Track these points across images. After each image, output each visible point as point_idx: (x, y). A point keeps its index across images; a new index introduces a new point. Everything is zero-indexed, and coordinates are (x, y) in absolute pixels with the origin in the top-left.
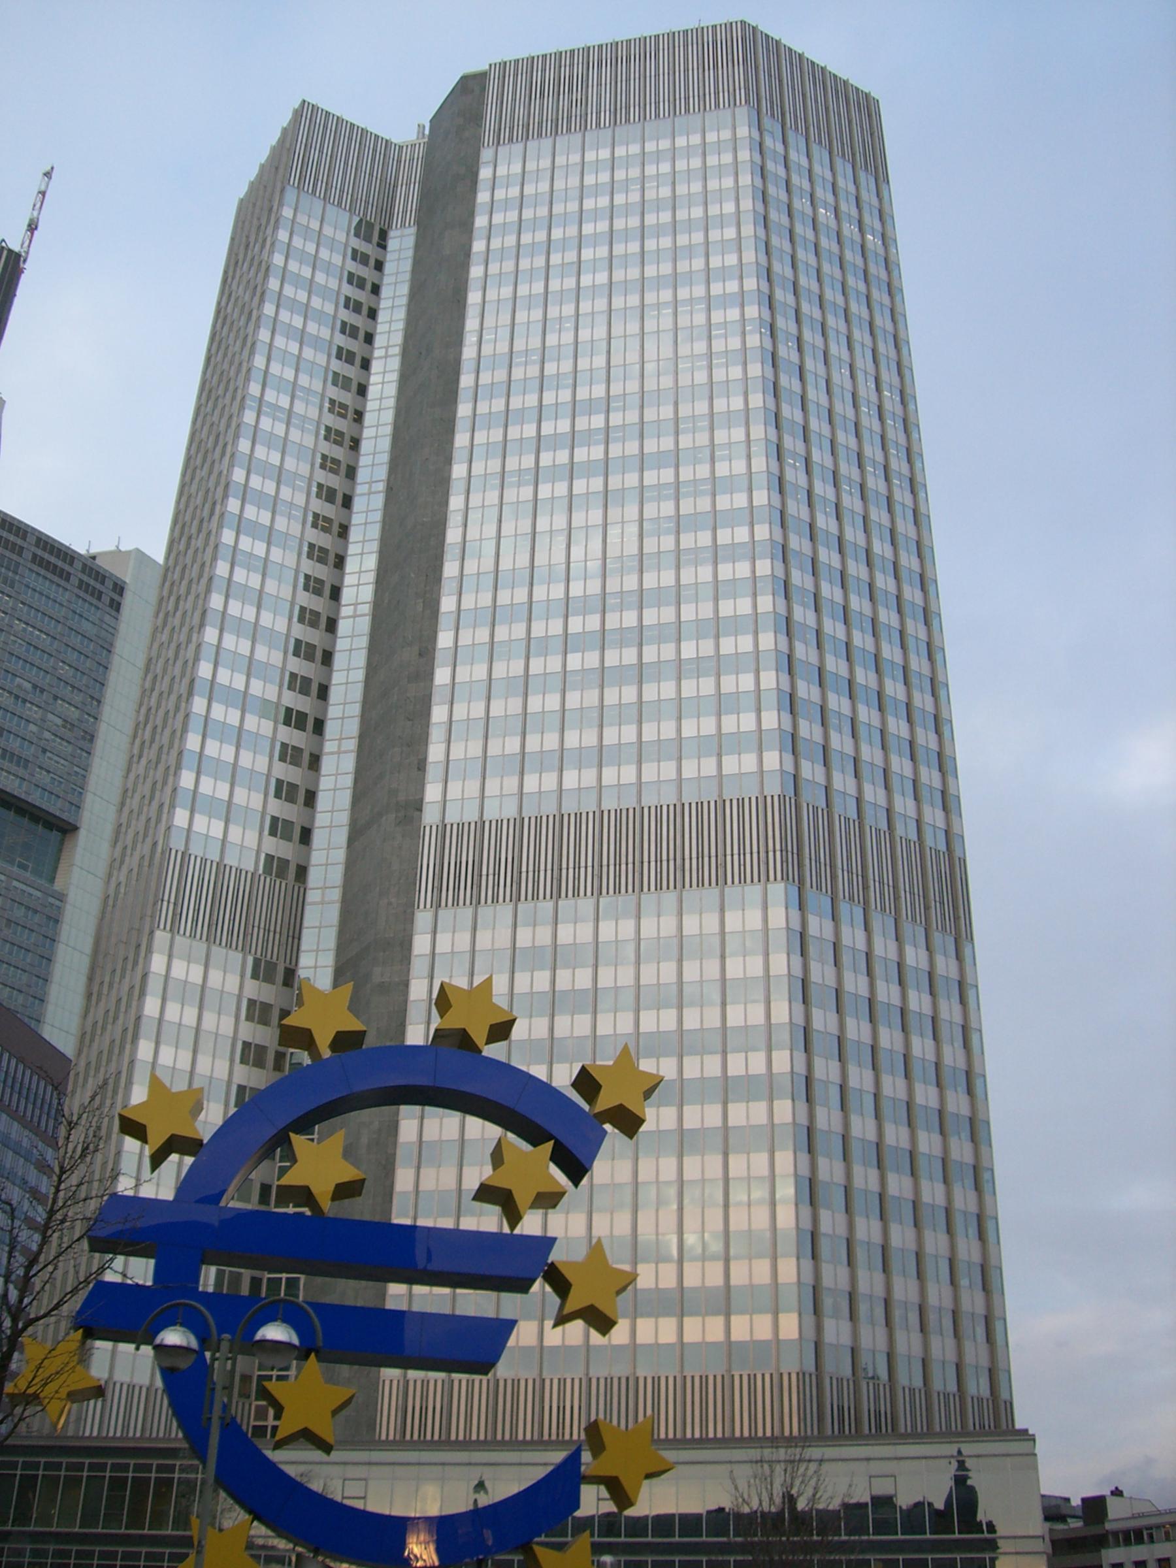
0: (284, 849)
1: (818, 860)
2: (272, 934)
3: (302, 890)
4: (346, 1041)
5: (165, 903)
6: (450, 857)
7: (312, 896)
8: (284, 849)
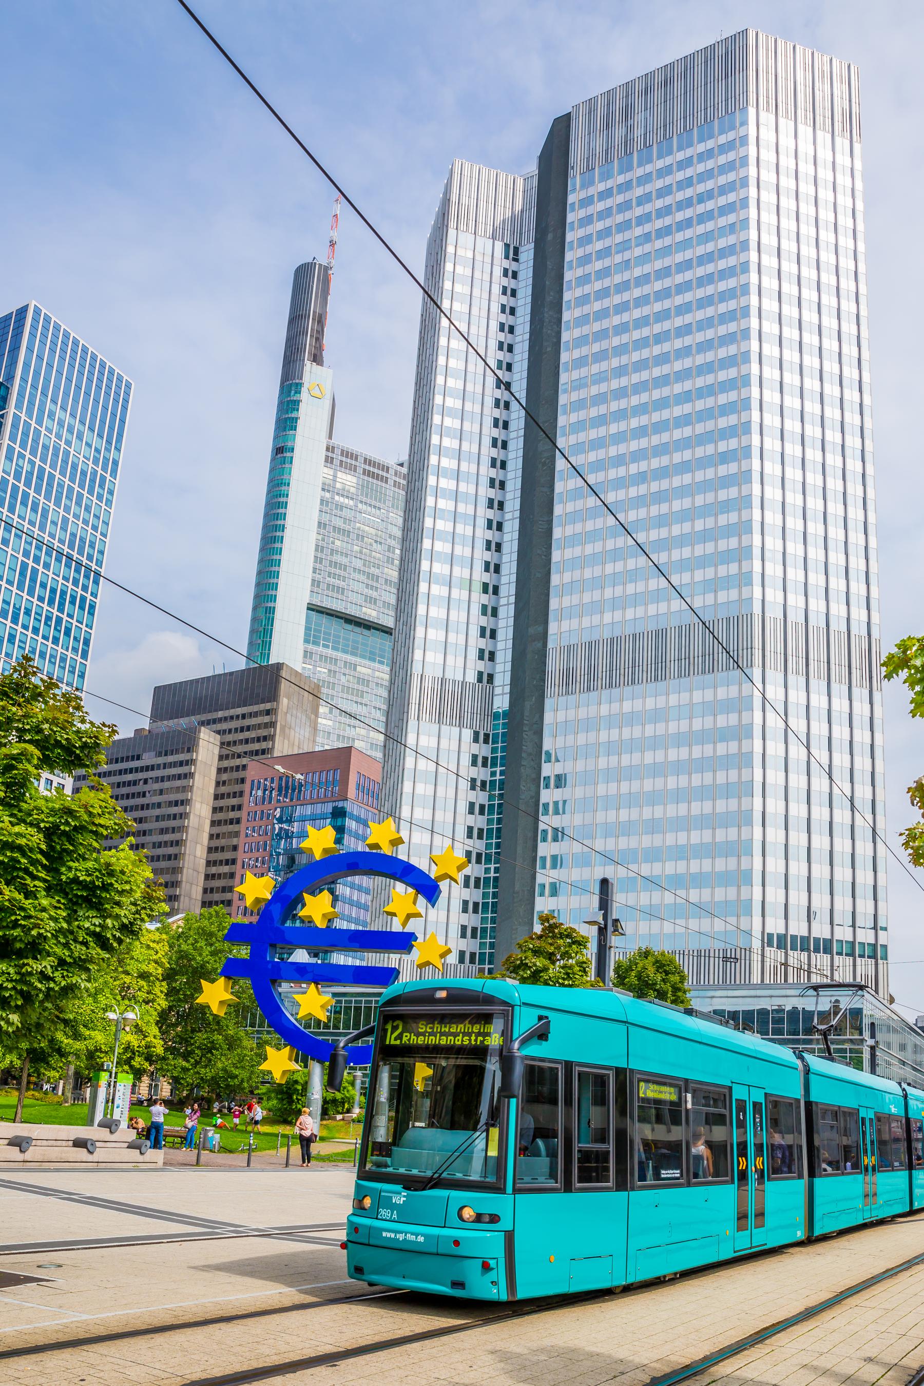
7: (498, 691)
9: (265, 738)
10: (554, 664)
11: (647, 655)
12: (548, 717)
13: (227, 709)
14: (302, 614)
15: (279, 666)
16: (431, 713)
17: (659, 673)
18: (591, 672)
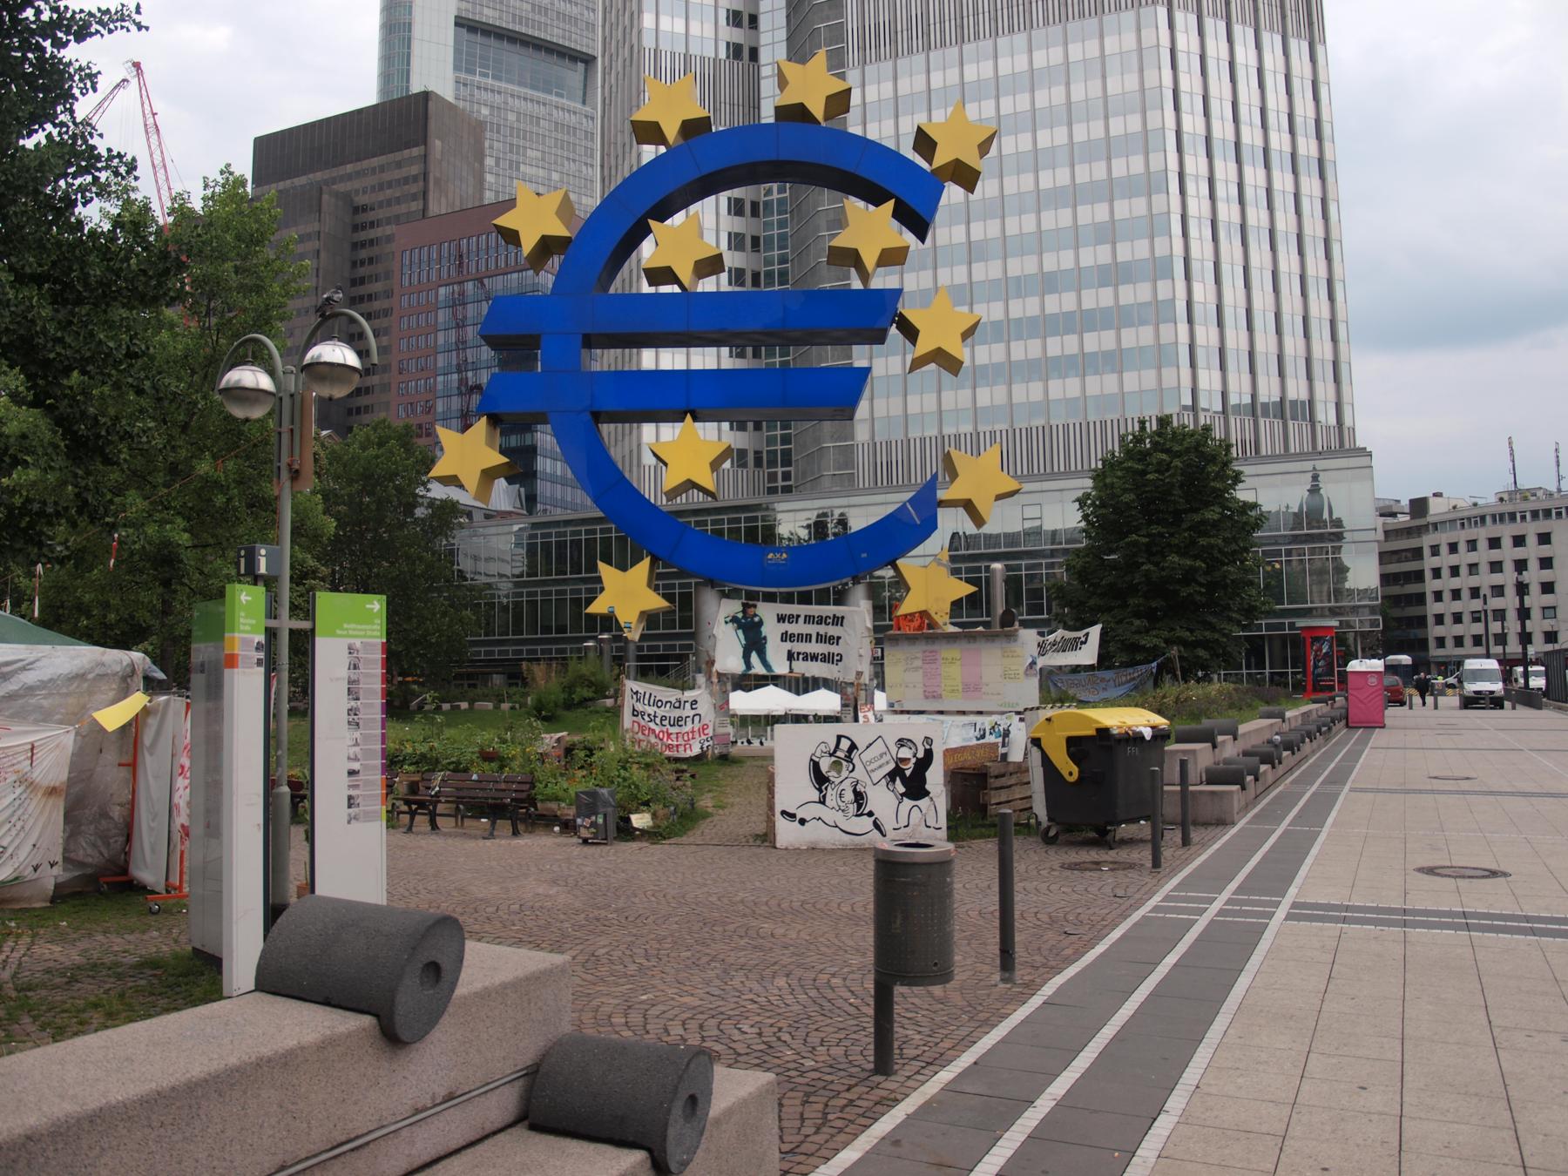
0: (738, 36)
4: (694, 129)
6: (870, 21)
8: (738, 36)
9: (414, 197)
13: (358, 160)
14: (448, 33)
15: (426, 96)
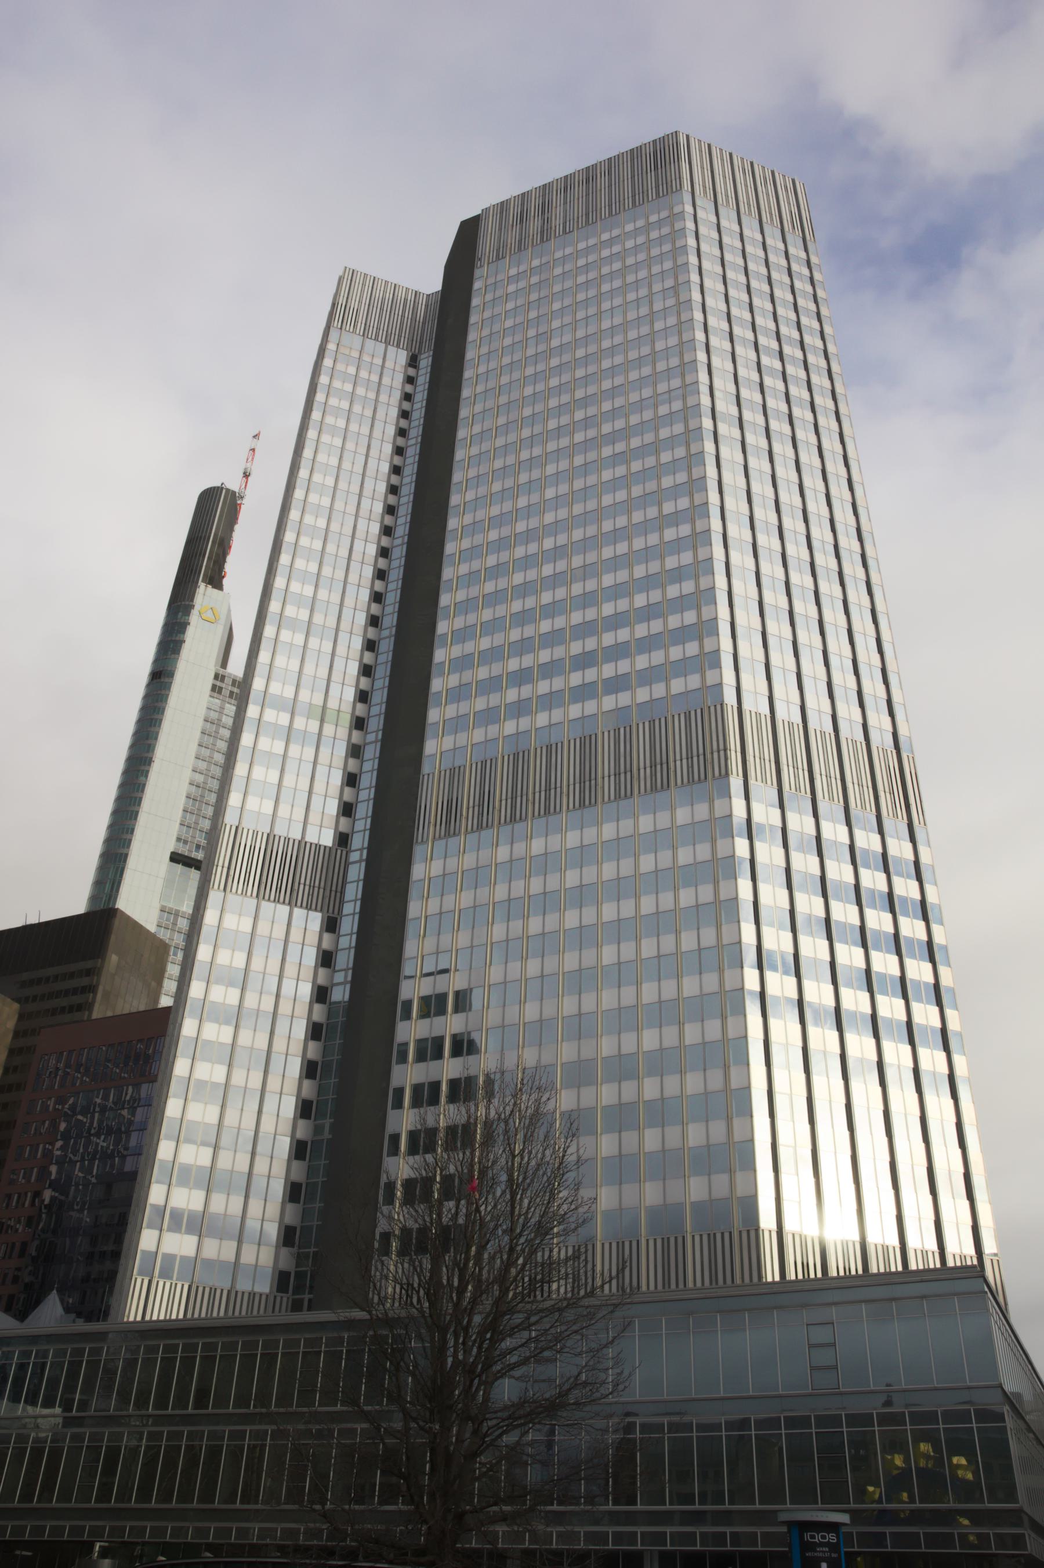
1: (762, 759)
2: (316, 889)
3: (344, 853)
5: (219, 869)
10: (431, 796)
11: (568, 769)
12: (418, 871)
16: (246, 882)
17: (586, 797)
18: (484, 802)
